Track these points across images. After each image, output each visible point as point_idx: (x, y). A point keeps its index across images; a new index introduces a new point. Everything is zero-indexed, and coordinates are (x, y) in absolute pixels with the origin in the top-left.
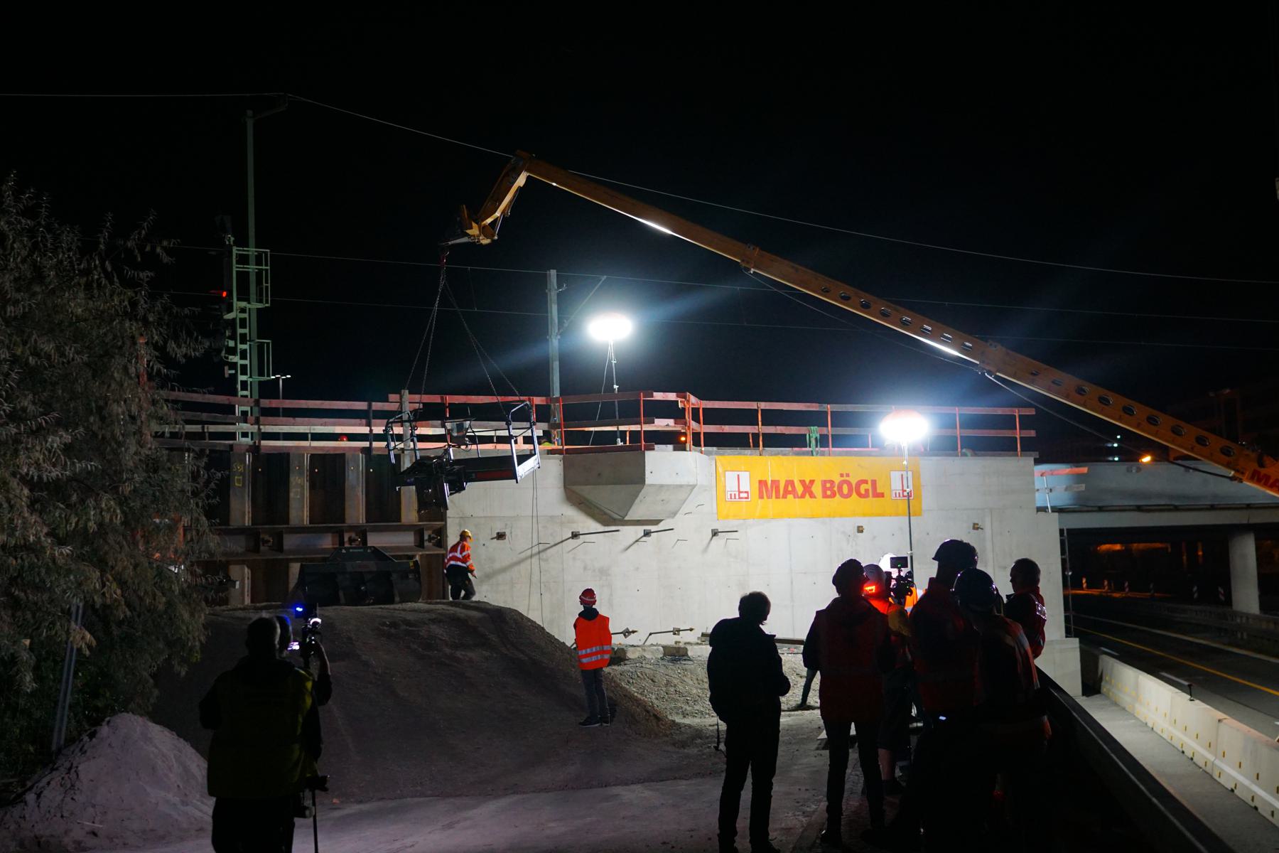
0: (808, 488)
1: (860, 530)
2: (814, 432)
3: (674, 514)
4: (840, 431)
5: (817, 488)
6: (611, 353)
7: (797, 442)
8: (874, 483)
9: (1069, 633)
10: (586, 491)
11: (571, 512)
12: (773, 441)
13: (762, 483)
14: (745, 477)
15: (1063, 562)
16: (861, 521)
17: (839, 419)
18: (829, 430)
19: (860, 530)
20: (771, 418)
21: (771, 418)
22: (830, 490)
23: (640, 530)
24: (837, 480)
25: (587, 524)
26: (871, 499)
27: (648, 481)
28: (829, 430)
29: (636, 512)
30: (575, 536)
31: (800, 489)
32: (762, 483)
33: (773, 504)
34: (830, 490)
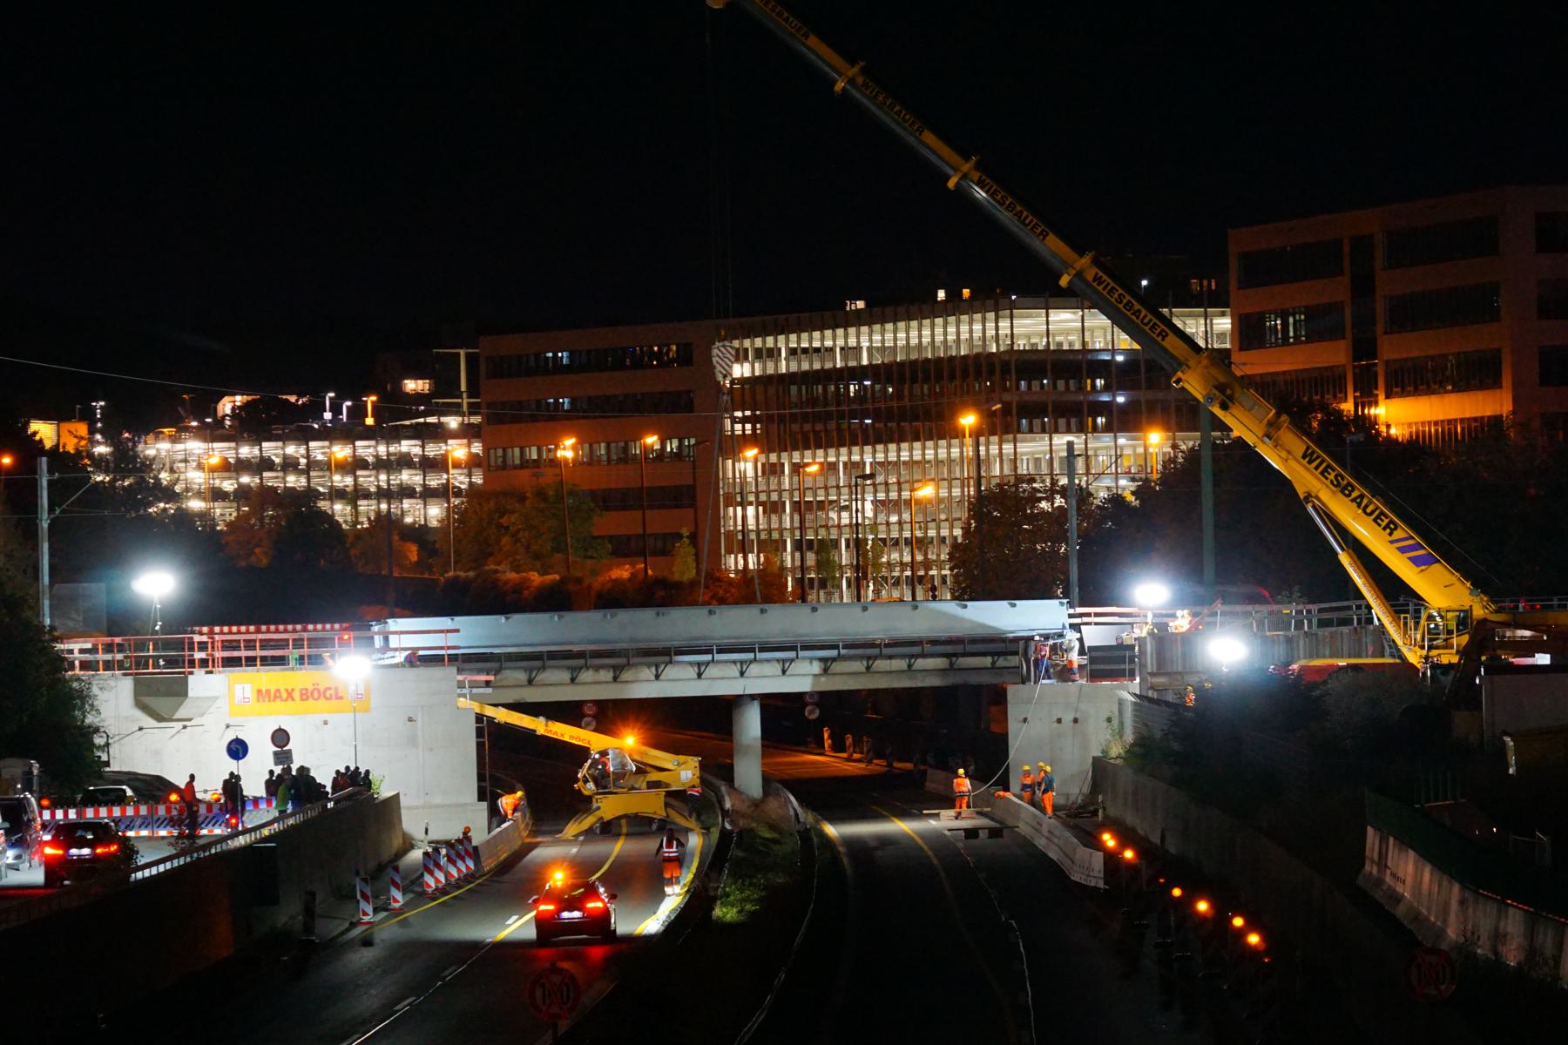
0: (290, 694)
1: (326, 723)
2: (293, 654)
3: (202, 715)
4: (314, 651)
5: (296, 695)
6: (156, 600)
7: (280, 661)
8: (336, 690)
9: (481, 798)
10: (149, 701)
11: (138, 714)
12: (266, 661)
13: (259, 692)
14: (248, 688)
15: (480, 746)
16: (326, 717)
17: (313, 642)
18: (305, 651)
19: (326, 723)
20: (265, 644)
21: (265, 644)
22: (305, 695)
23: (181, 724)
24: (310, 688)
25: (148, 721)
26: (334, 702)
27: (190, 694)
28: (305, 651)
29: (180, 714)
30: (141, 729)
31: (284, 695)
32: (259, 692)
33: (267, 705)
34: (305, 695)
